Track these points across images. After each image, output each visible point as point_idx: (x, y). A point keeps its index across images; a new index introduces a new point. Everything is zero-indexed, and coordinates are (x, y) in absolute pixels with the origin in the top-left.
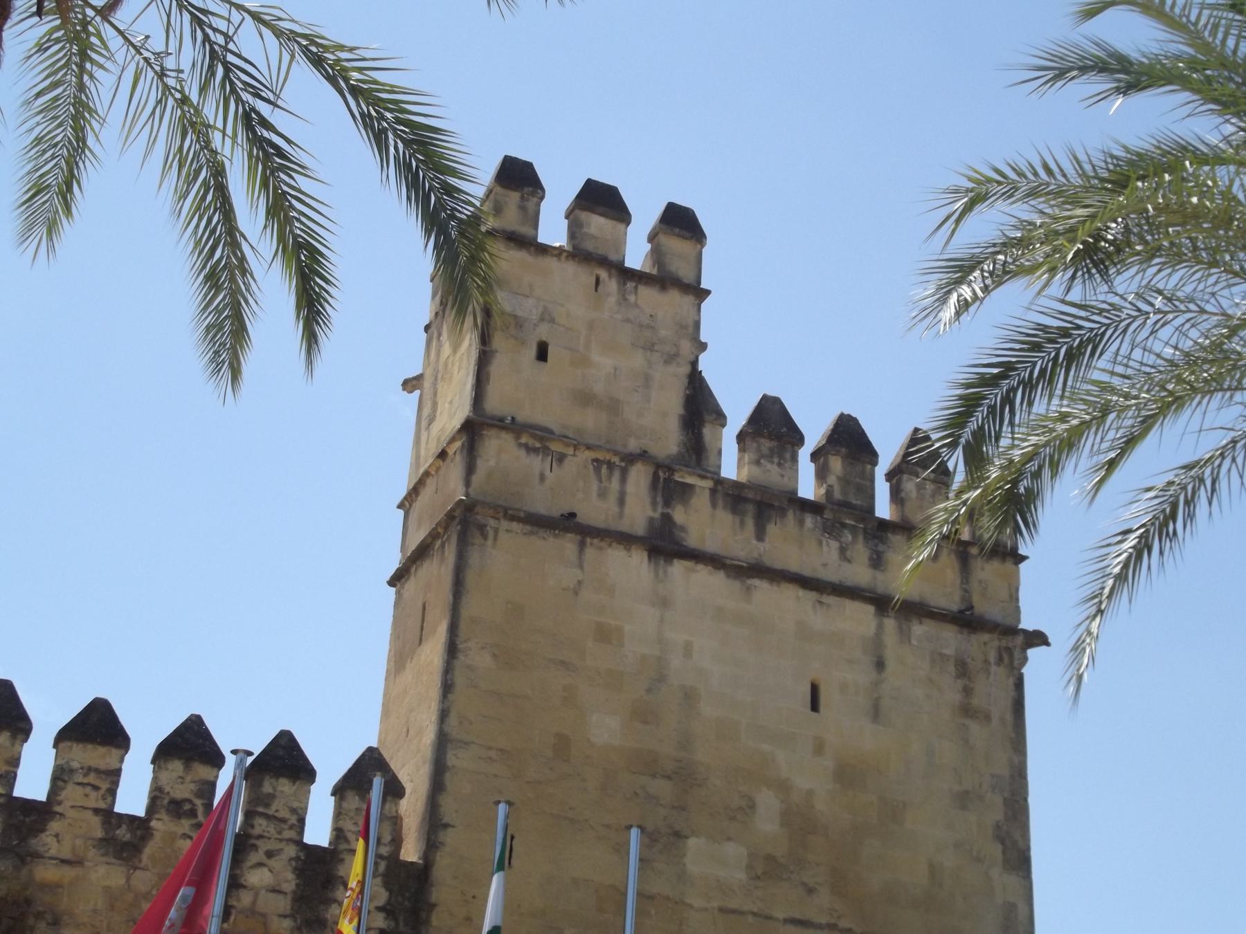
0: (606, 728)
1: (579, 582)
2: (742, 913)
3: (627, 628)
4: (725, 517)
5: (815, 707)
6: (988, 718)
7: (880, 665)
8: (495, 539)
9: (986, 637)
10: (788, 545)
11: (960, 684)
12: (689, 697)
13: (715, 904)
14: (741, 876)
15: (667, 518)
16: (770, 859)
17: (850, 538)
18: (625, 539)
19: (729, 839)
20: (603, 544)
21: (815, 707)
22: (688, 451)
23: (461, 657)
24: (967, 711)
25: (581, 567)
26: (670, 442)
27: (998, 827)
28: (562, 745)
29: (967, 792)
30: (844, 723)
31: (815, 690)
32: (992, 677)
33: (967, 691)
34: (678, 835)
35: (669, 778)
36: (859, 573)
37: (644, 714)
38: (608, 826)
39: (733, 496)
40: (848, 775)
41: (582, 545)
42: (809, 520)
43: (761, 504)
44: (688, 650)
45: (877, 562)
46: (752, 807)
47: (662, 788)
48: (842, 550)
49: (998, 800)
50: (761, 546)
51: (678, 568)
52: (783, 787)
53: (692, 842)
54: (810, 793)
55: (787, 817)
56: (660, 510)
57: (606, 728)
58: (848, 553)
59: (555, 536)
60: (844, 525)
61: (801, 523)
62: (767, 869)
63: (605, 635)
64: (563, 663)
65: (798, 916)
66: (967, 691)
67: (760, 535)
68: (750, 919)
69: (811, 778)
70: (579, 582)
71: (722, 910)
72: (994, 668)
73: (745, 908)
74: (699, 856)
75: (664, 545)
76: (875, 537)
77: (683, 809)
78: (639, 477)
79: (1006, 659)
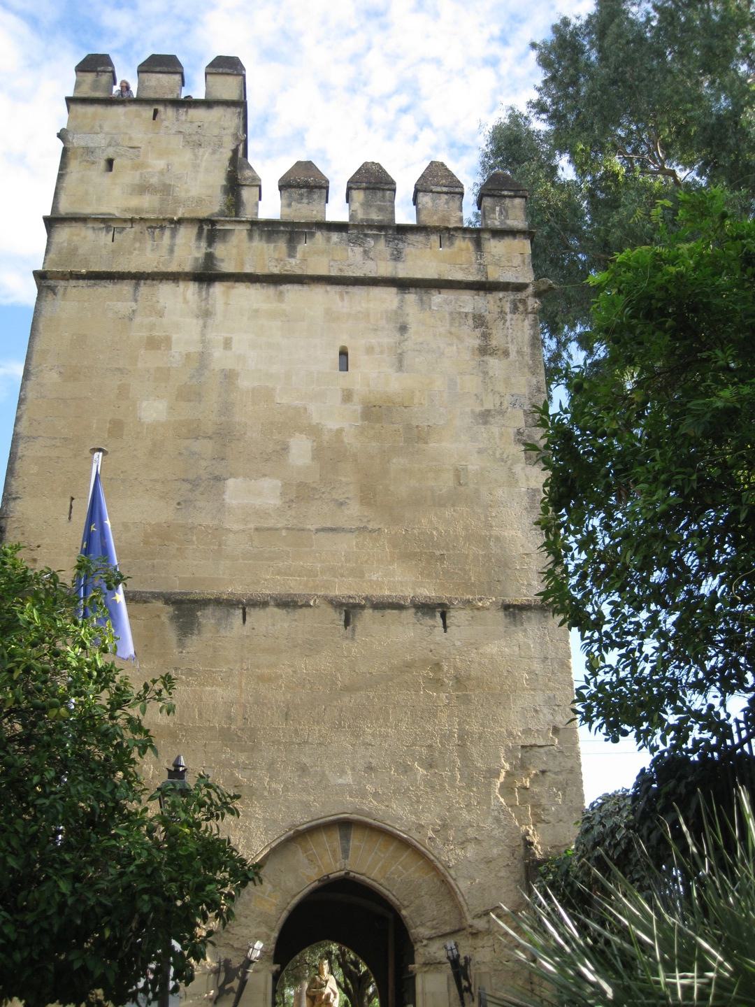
0: (154, 410)
1: (133, 311)
2: (277, 529)
3: (174, 337)
4: (259, 245)
5: (344, 366)
6: (506, 353)
7: (403, 329)
8: (64, 294)
9: (501, 295)
10: (317, 256)
11: (478, 332)
12: (229, 377)
13: (252, 526)
14: (278, 502)
15: (210, 257)
16: (302, 485)
17: (372, 243)
18: (174, 277)
19: (265, 475)
20: (155, 282)
21: (344, 366)
22: (228, 208)
23: (33, 378)
24: (484, 350)
25: (136, 301)
26: (214, 204)
27: (519, 433)
28: (117, 428)
29: (489, 411)
30: (372, 374)
31: (344, 353)
32: (508, 323)
33: (485, 336)
34: (218, 479)
35: (210, 438)
36: (384, 269)
37: (189, 394)
38: (156, 481)
39: (269, 229)
40: (375, 412)
41: (137, 285)
42: (335, 237)
43: (288, 232)
44: (227, 344)
45: (397, 257)
46: (285, 449)
47: (205, 447)
48: (365, 252)
49: (520, 413)
50: (293, 261)
51: (218, 289)
52: (314, 431)
53: (231, 482)
54: (341, 431)
55: (318, 453)
56: (204, 251)
57: (154, 410)
58: (371, 254)
59: (114, 284)
60: (366, 235)
61: (328, 240)
62: (299, 493)
63: (154, 344)
64: (119, 369)
65: (329, 525)
66: (485, 336)
67: (292, 252)
68: (284, 533)
69: (337, 419)
70: (133, 311)
71: (257, 529)
72: (509, 317)
73: (279, 525)
74: (236, 492)
75: (206, 275)
76: (395, 239)
77: (223, 459)
78: (186, 236)
79: (521, 308)
